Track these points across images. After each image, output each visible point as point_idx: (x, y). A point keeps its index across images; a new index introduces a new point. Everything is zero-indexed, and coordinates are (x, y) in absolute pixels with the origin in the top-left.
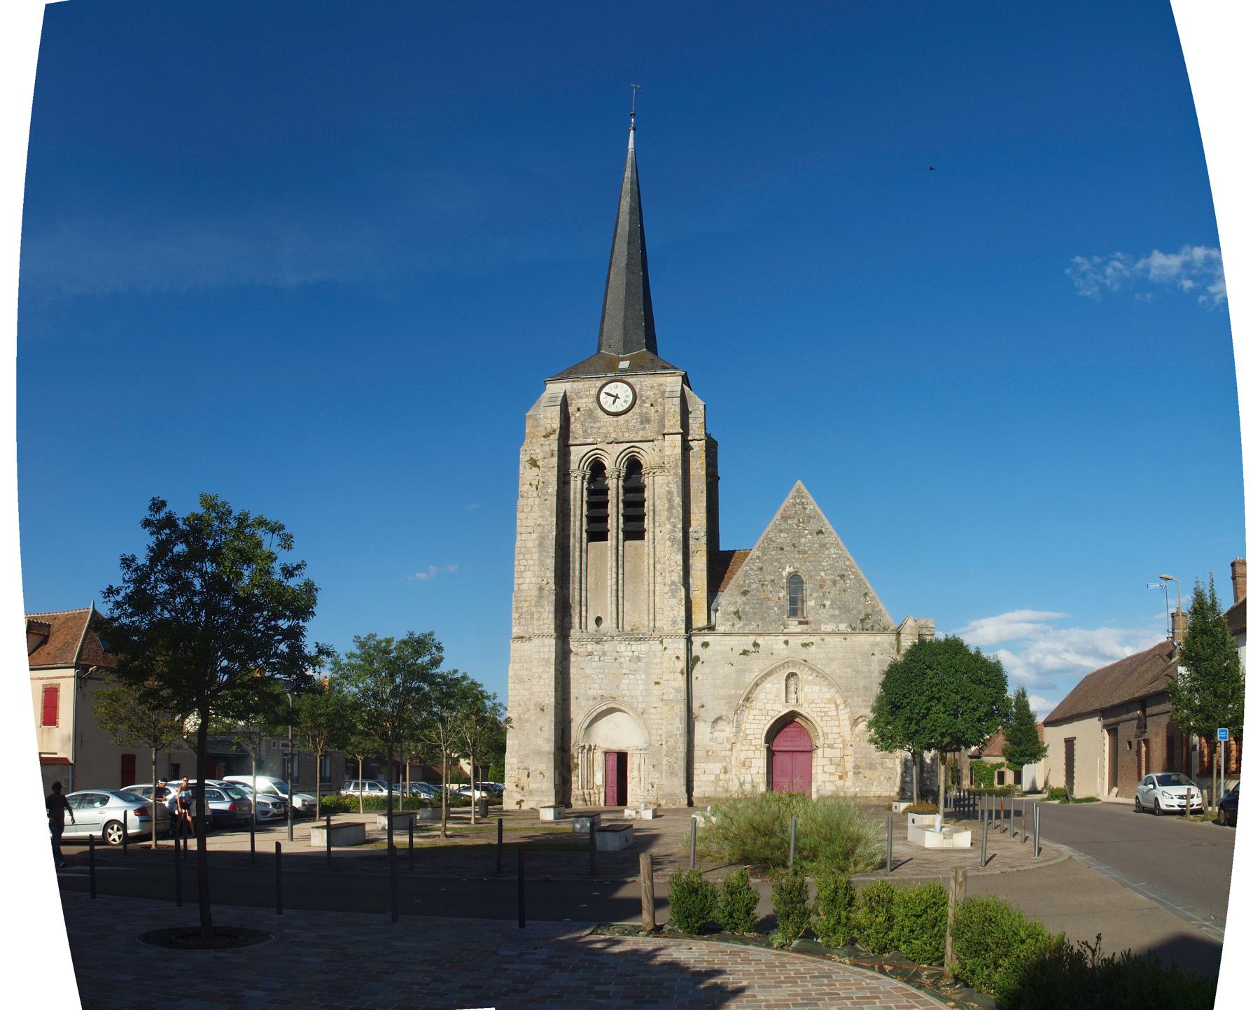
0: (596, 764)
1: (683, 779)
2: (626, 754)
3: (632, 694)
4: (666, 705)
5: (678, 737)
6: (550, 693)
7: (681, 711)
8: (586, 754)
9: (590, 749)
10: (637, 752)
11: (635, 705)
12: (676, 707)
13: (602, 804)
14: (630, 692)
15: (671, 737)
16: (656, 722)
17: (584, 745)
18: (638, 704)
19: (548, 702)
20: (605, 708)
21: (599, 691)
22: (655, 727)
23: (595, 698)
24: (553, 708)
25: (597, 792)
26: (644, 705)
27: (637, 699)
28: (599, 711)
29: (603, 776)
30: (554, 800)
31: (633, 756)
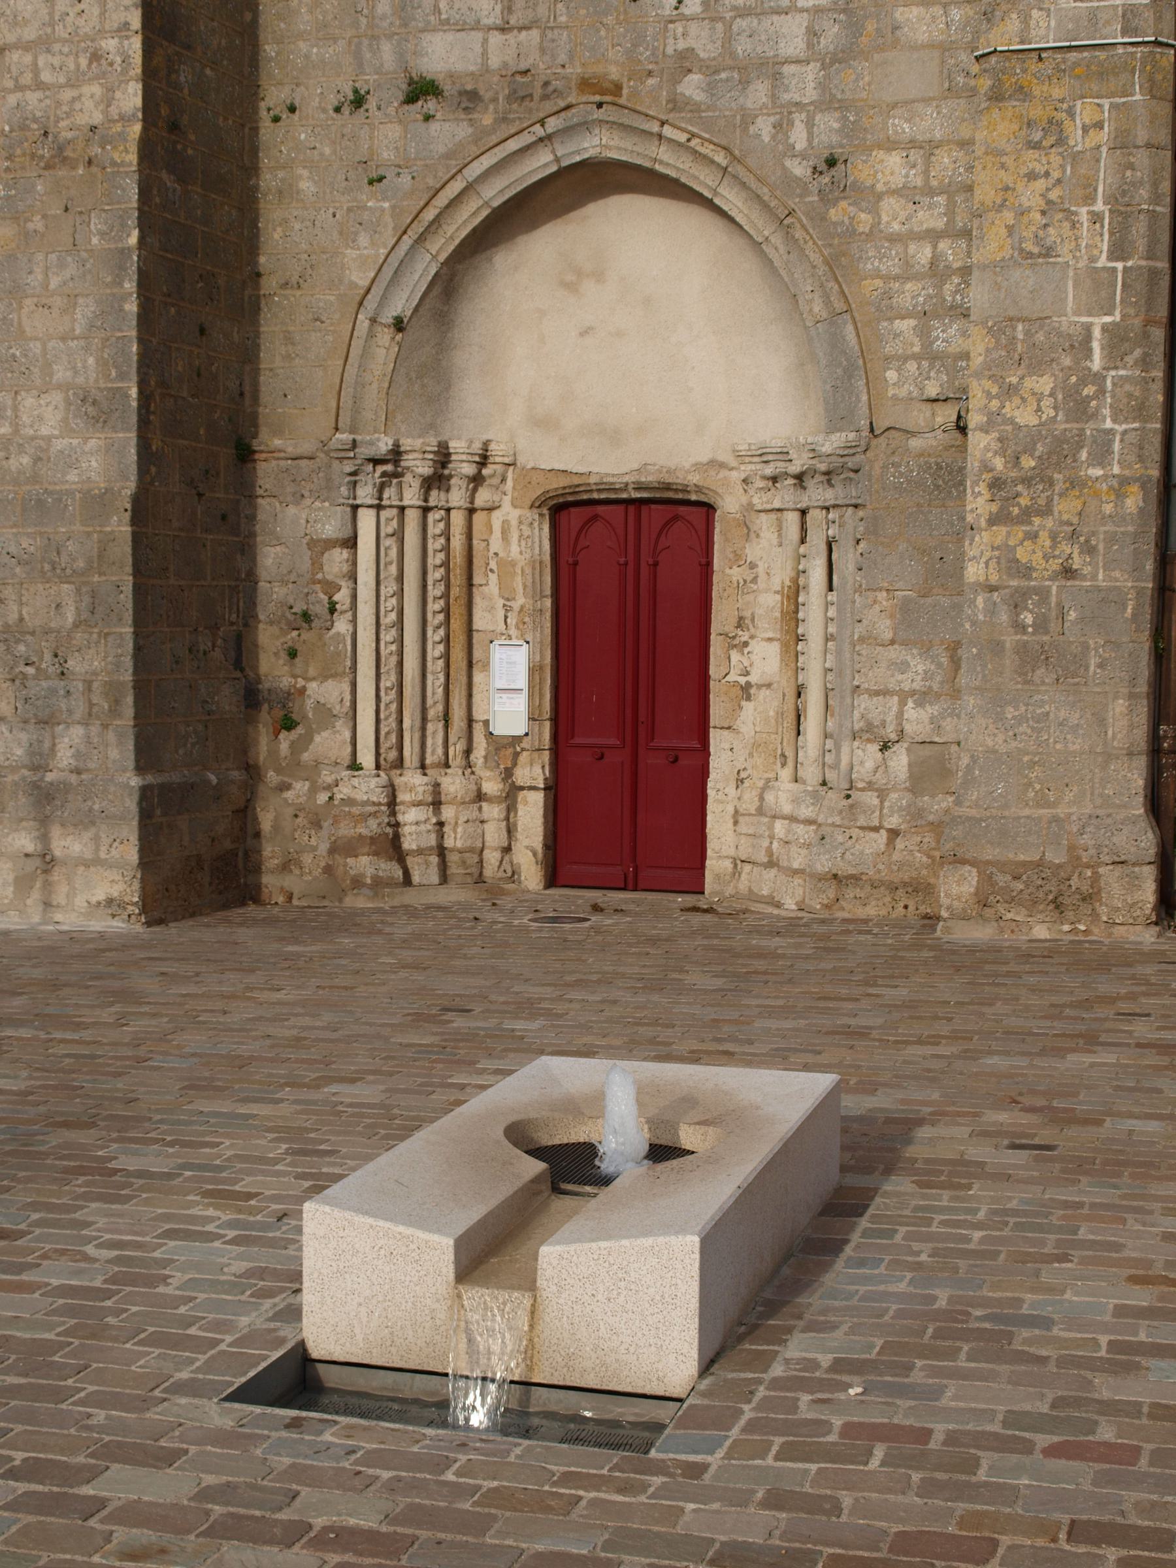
0: (489, 589)
1: (1120, 706)
2: (708, 508)
3: (743, 47)
4: (997, 96)
5: (1097, 363)
6: (110, 44)
7: (1122, 143)
8: (412, 517)
9: (437, 480)
10: (785, 495)
11: (764, 127)
12: (1085, 112)
13: (531, 876)
14: (729, 38)
15: (1036, 363)
16: (923, 254)
17: (396, 454)
18: (782, 127)
19: (97, 118)
20: (541, 164)
21: (495, 38)
22: (912, 293)
23: (470, 99)
24: (132, 157)
25: (492, 787)
26: (828, 124)
27: (777, 77)
28: (496, 192)
29: (534, 670)
30: (131, 854)
31: (748, 532)
